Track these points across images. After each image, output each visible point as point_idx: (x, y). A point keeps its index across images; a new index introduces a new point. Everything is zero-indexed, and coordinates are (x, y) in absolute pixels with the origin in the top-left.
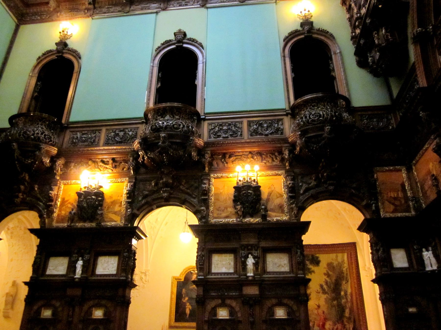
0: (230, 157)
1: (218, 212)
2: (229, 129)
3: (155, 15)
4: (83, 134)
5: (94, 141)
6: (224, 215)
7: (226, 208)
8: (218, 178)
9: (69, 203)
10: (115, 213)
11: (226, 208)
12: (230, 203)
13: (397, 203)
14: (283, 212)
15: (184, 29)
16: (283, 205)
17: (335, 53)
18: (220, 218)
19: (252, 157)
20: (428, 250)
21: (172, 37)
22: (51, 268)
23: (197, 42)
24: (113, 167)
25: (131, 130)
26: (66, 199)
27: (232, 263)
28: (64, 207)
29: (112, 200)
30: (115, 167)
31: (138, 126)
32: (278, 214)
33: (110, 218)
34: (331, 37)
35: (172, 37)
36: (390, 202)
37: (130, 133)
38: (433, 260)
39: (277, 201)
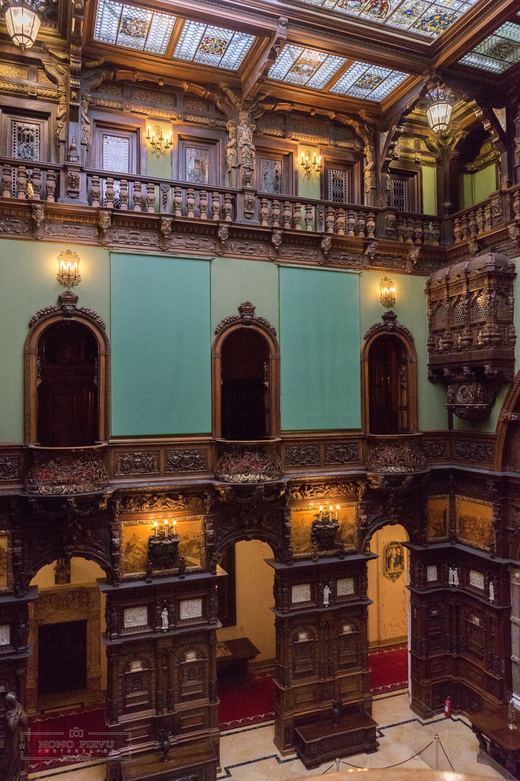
0: (309, 489)
1: (297, 547)
2: (307, 453)
3: (208, 263)
4: (135, 457)
5: (153, 466)
6: (303, 549)
7: (305, 542)
8: (297, 511)
9: (137, 548)
10: (194, 556)
11: (305, 542)
12: (308, 537)
13: (438, 528)
14: (353, 542)
16: (354, 536)
17: (411, 362)
18: (301, 552)
19: (329, 488)
20: (454, 570)
22: (128, 621)
24: (184, 503)
25: (198, 453)
26: (131, 544)
27: (309, 593)
28: (131, 554)
29: (188, 541)
30: (187, 503)
31: (206, 447)
32: (349, 545)
33: (189, 562)
34: (411, 340)
36: (434, 529)
37: (198, 456)
38: (456, 578)
39: (350, 532)
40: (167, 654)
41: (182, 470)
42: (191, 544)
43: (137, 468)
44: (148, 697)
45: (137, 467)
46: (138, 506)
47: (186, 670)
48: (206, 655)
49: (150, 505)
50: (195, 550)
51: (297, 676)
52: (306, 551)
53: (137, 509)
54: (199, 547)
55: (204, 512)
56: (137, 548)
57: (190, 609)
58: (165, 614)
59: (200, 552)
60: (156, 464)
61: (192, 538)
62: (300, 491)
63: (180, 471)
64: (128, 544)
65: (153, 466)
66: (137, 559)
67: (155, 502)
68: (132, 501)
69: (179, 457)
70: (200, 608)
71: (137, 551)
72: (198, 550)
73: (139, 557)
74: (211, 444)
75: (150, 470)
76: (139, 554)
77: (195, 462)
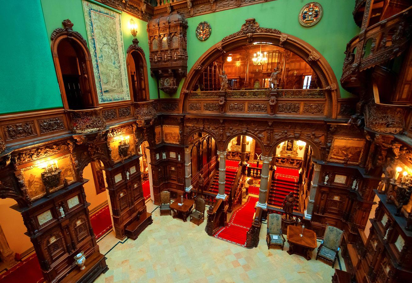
4: (17, 127)
5: (32, 131)
6: (116, 159)
10: (69, 176)
12: (118, 153)
15: (70, 19)
17: (145, 67)
21: (61, 26)
22: (41, 221)
23: (82, 39)
27: (121, 177)
28: (33, 186)
29: (64, 170)
30: (59, 149)
31: (62, 115)
35: (61, 26)
40: (67, 227)
41: (50, 131)
42: (66, 170)
43: (22, 134)
44: (63, 250)
45: (20, 133)
46: (29, 157)
47: (78, 230)
48: (86, 219)
49: (37, 155)
50: (69, 173)
51: (122, 210)
52: (118, 159)
53: (29, 159)
54: (71, 171)
55: (69, 152)
56: (35, 182)
57: (73, 202)
58: (61, 210)
59: (72, 173)
60: (33, 129)
61: (66, 168)
62: (111, 133)
63: (50, 132)
64: (29, 181)
65: (32, 131)
66: (38, 188)
67: (40, 153)
68: (24, 155)
69: (48, 123)
70: (78, 200)
71: (36, 183)
72: (71, 173)
73: (38, 186)
74: (64, 113)
75: (30, 134)
76: (38, 185)
77: (58, 125)
